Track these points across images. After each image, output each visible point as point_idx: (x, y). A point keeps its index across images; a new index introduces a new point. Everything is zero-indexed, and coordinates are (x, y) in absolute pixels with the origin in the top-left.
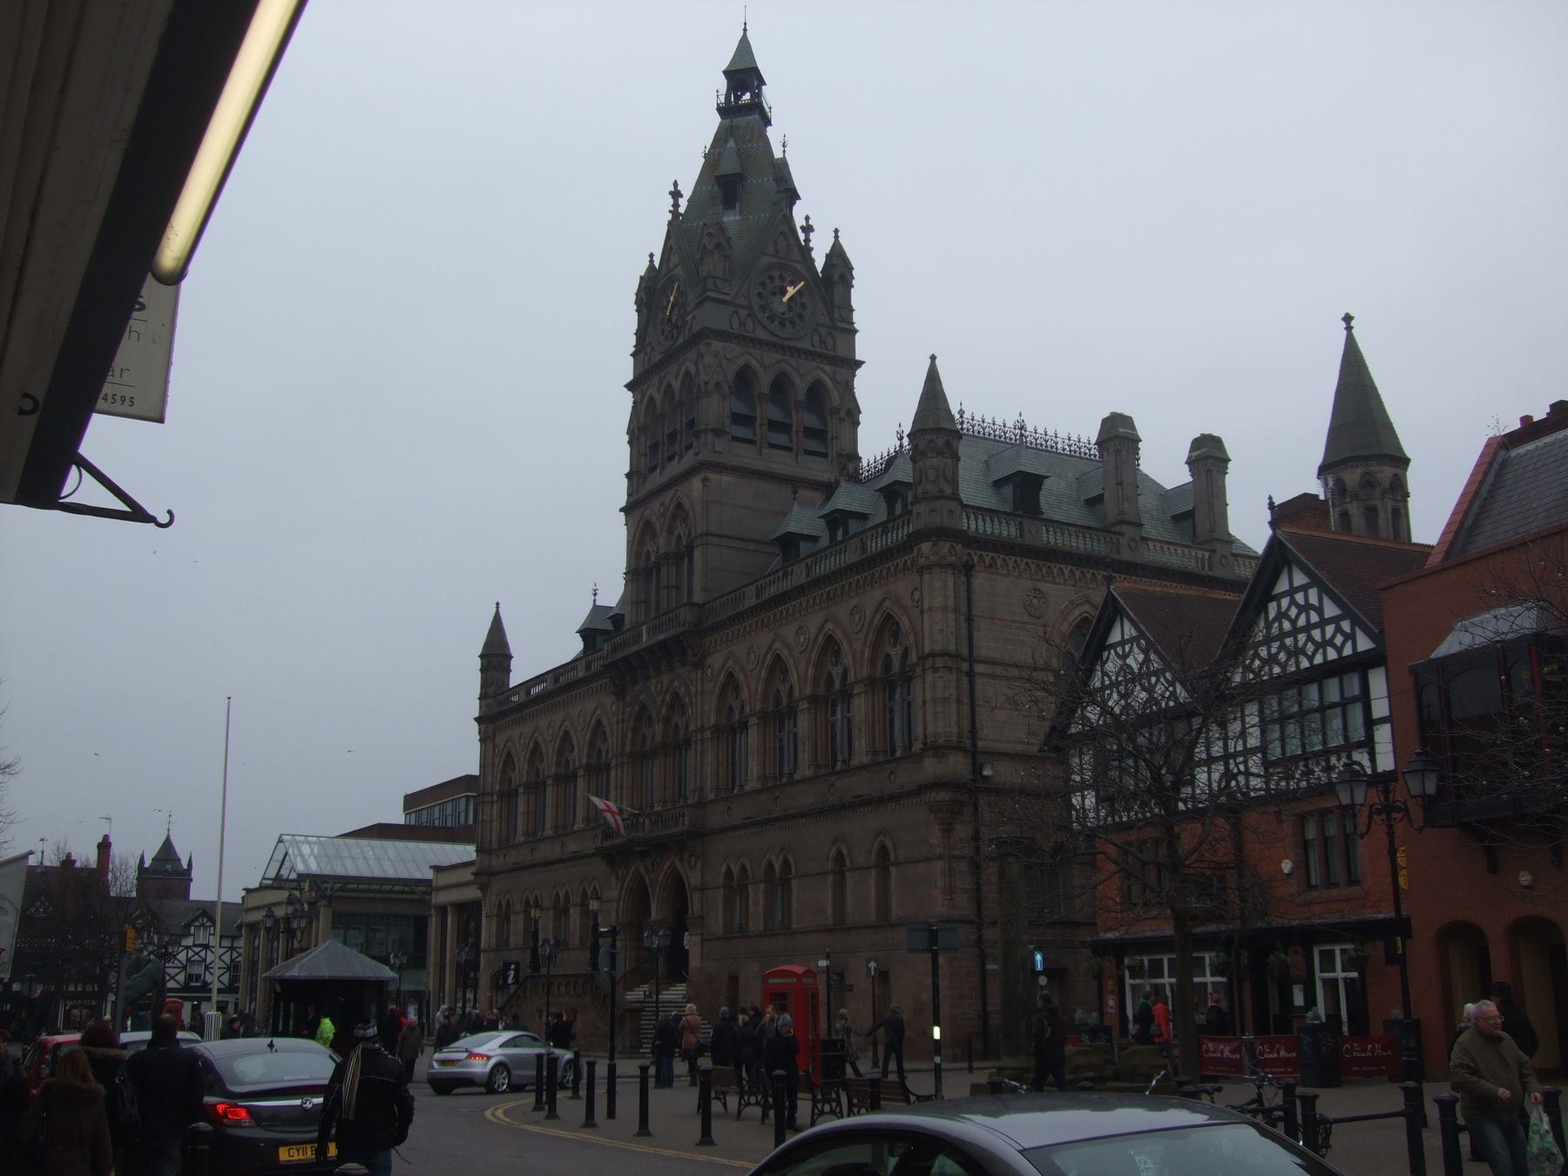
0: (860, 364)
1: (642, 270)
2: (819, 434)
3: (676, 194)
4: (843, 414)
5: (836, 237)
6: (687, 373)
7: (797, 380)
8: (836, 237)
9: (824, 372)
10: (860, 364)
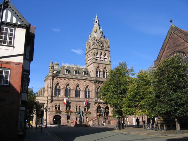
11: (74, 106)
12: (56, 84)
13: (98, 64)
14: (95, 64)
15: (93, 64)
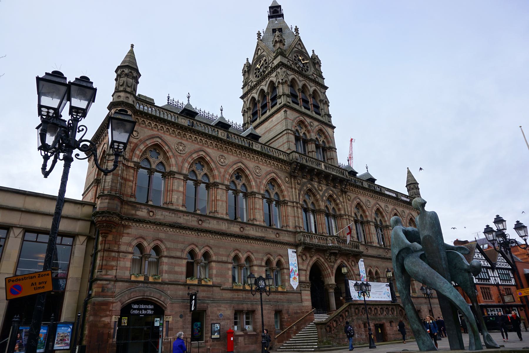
0: (326, 88)
1: (245, 62)
2: (316, 107)
3: (259, 34)
4: (324, 101)
5: (313, 52)
6: (272, 82)
7: (309, 87)
8: (313, 52)
9: (318, 89)
10: (326, 88)
11: (224, 259)
12: (142, 147)
13: (296, 115)
14: (289, 112)
15: (284, 109)
